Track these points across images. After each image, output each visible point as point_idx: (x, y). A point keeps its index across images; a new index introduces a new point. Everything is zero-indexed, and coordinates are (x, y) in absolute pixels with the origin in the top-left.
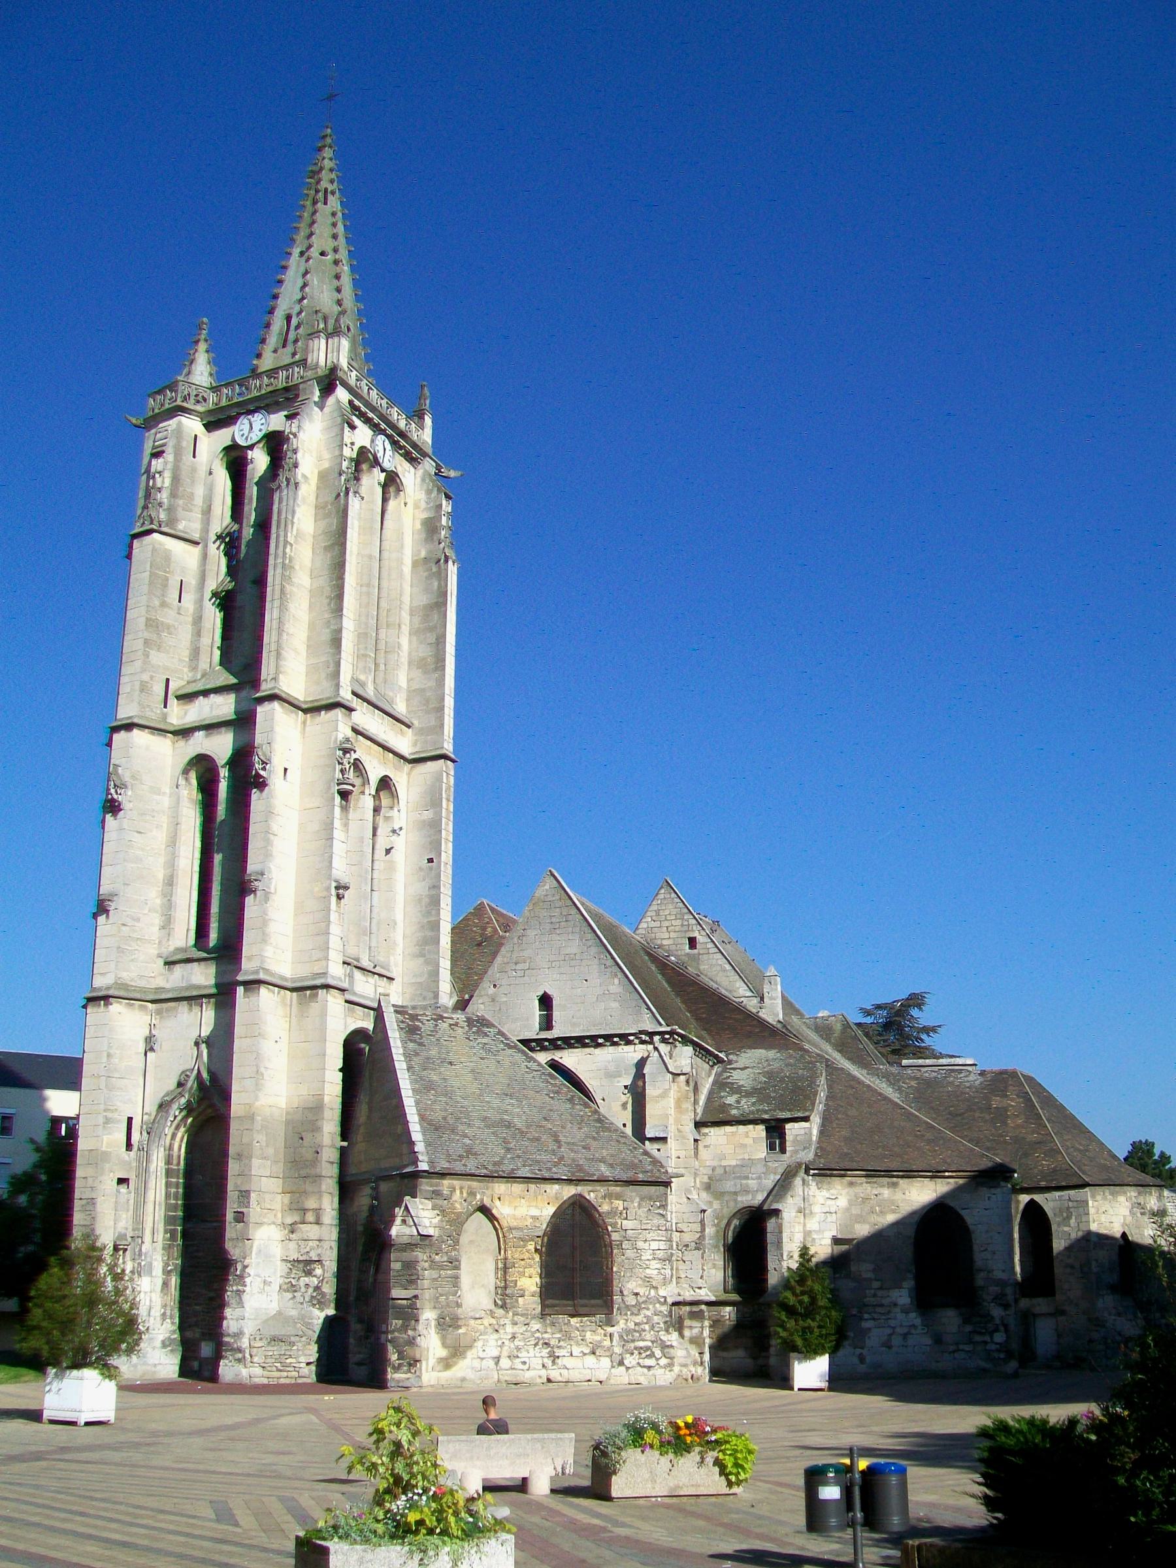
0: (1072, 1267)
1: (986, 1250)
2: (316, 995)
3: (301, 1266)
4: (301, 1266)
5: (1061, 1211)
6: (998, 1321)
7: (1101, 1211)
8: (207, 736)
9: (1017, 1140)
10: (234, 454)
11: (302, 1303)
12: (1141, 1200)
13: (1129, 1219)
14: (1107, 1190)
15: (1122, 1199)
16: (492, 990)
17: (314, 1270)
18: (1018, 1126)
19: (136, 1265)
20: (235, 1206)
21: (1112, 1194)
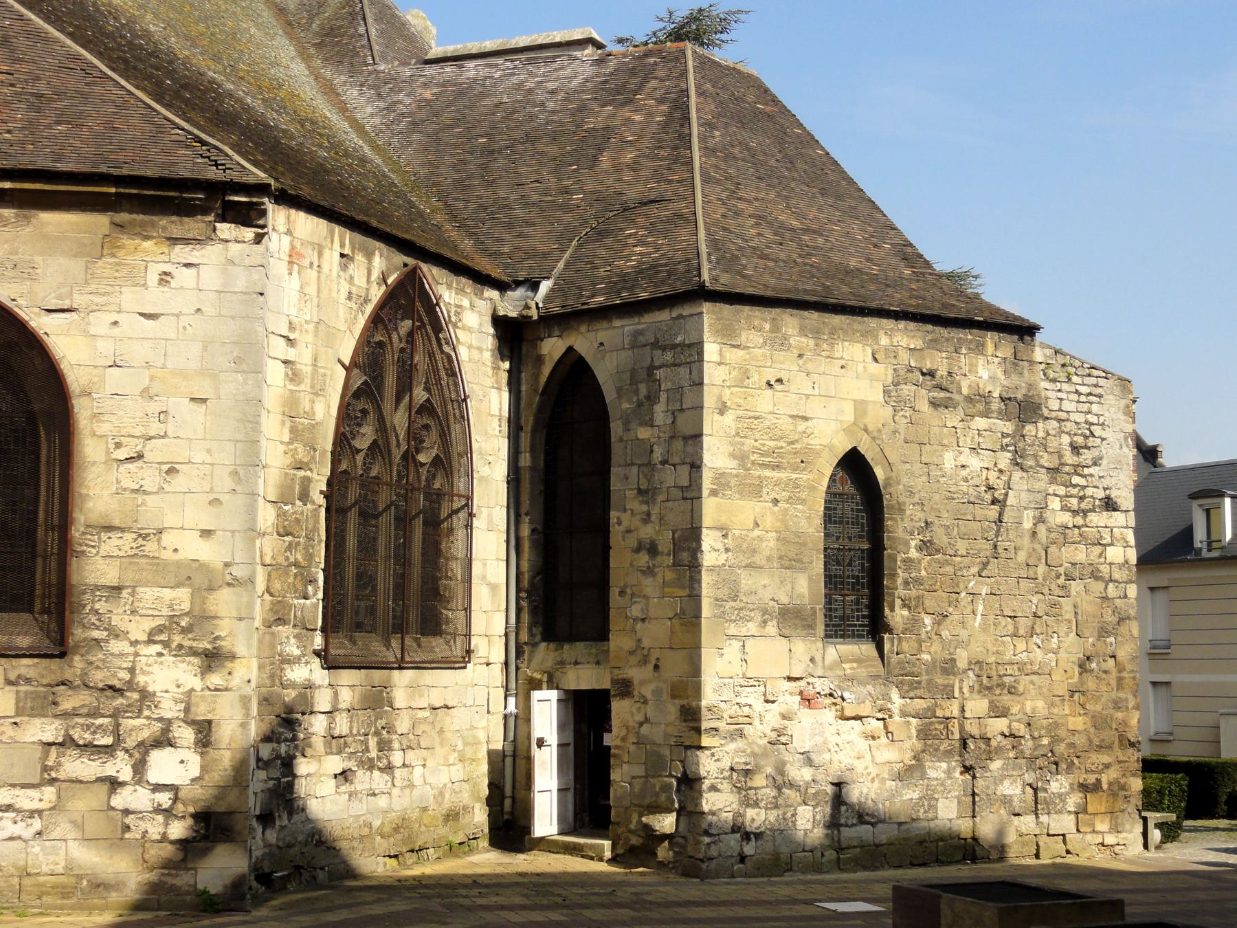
0: (653, 550)
1: (140, 456)
5: (634, 381)
6: (170, 709)
7: (756, 379)
9: (599, 198)
12: (938, 361)
13: (880, 414)
14: (790, 321)
15: (854, 352)
18: (618, 167)
21: (816, 334)
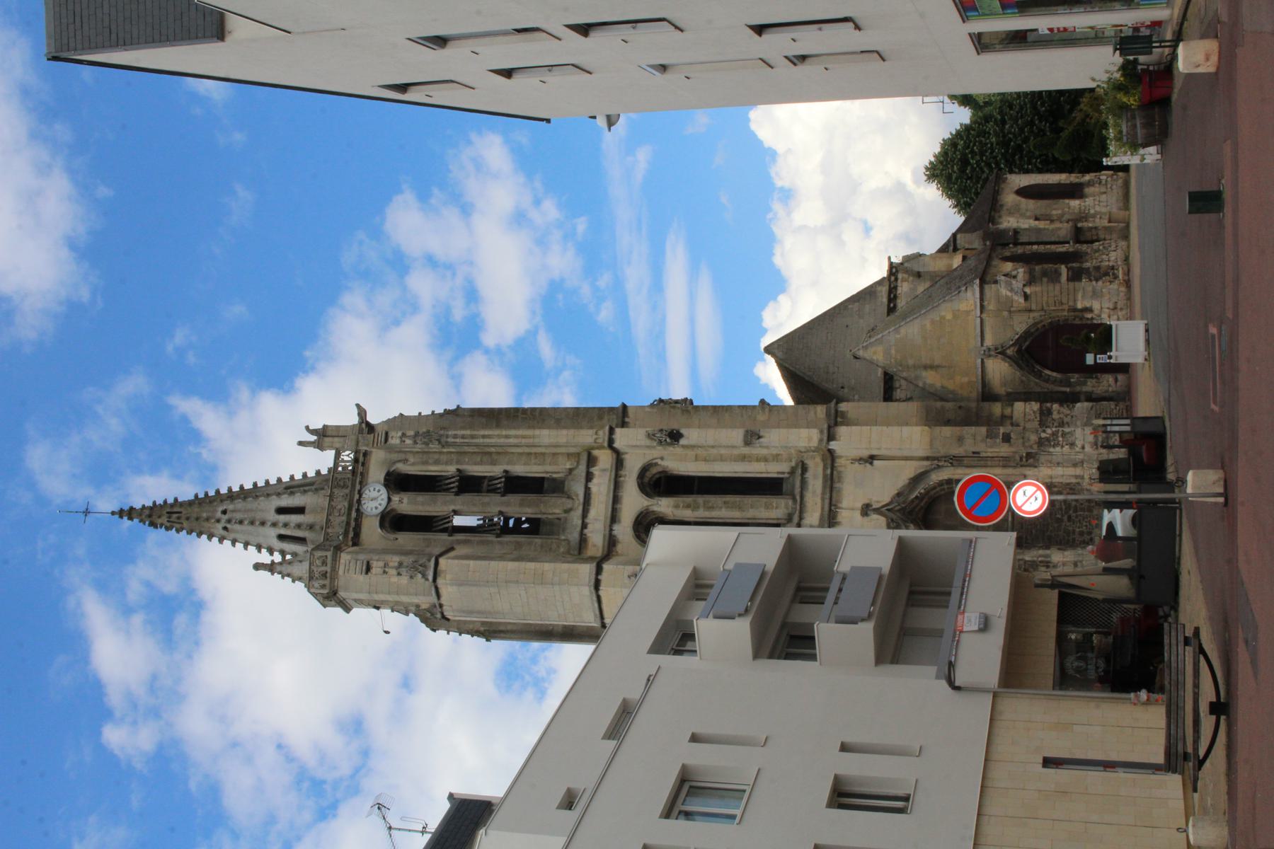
2: (841, 411)
3: (1043, 418)
4: (1043, 418)
8: (620, 522)
10: (388, 519)
11: (1072, 417)
16: (846, 390)
17: (1047, 407)
19: (1042, 564)
20: (998, 441)
